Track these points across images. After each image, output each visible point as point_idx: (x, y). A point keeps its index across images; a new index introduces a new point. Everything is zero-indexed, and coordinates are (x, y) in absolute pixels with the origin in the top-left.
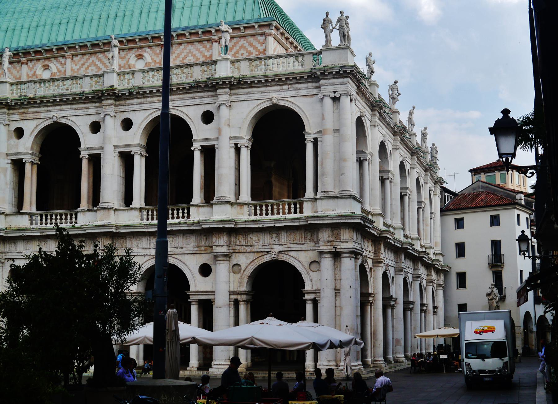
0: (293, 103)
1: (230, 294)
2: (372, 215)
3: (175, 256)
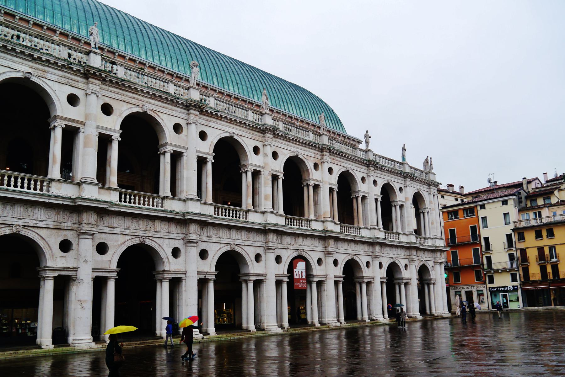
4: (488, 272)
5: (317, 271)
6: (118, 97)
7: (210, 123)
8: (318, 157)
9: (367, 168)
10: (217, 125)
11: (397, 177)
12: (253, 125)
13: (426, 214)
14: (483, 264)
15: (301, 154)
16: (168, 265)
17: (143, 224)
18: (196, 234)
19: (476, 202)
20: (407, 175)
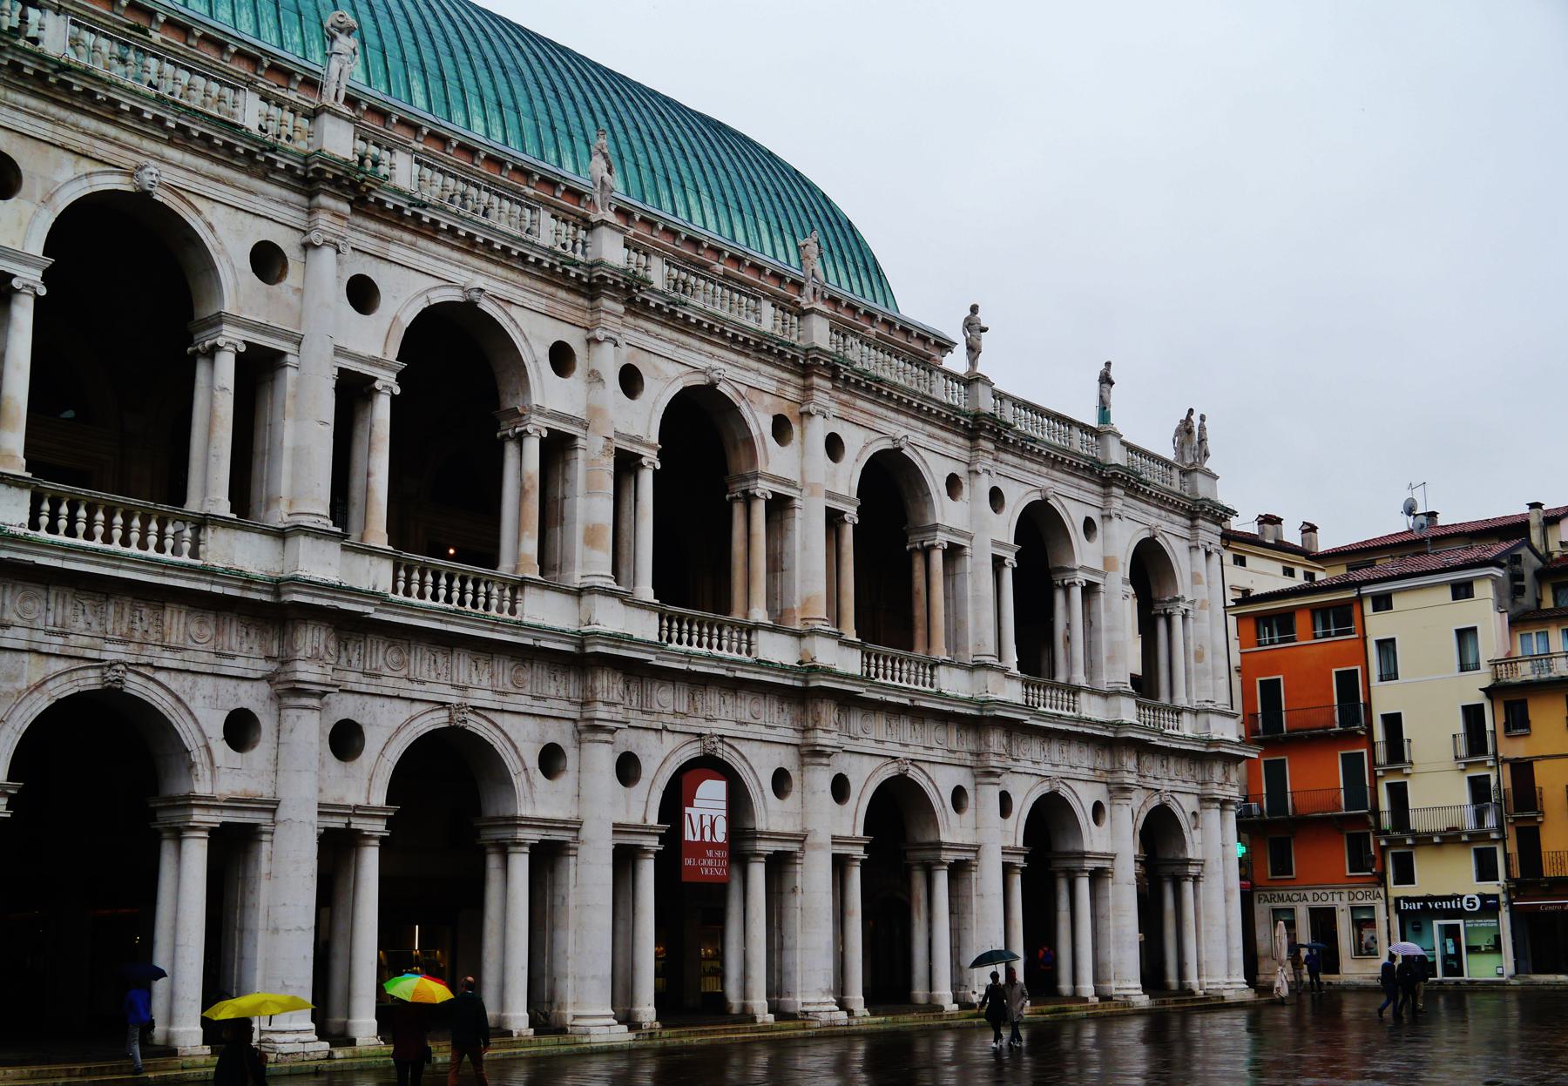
4: (1392, 842)
5: (771, 815)
6: (44, 130)
7: (392, 247)
8: (791, 393)
9: (968, 444)
10: (416, 255)
11: (1076, 480)
12: (551, 264)
13: (1178, 620)
14: (1376, 812)
15: (728, 381)
16: (208, 773)
17: (116, 618)
18: (321, 663)
19: (1358, 585)
20: (1114, 475)
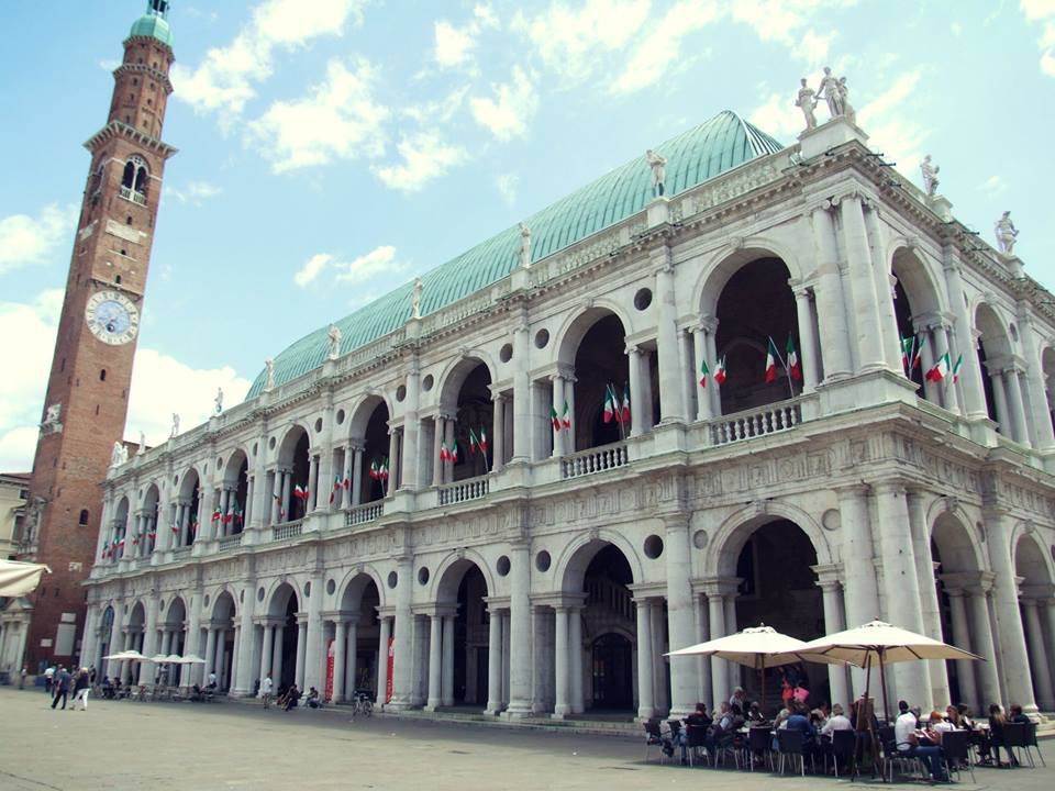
0: (765, 240)
1: (692, 586)
2: (968, 425)
3: (609, 528)
6: (226, 446)
11: (618, 272)
